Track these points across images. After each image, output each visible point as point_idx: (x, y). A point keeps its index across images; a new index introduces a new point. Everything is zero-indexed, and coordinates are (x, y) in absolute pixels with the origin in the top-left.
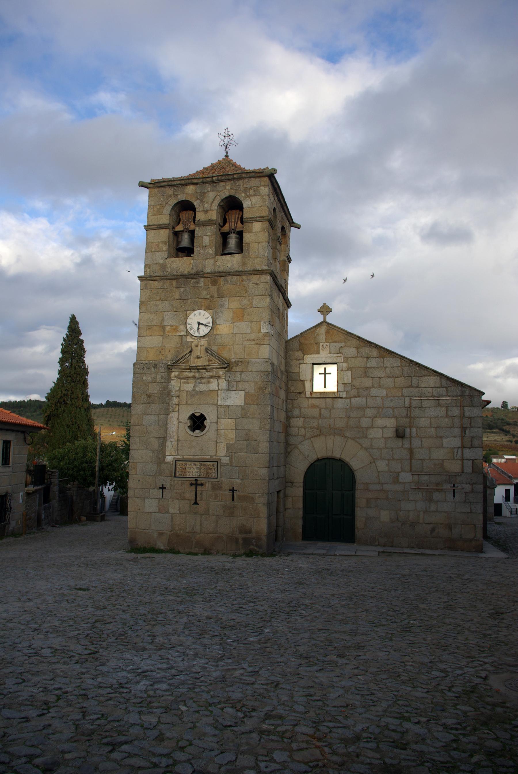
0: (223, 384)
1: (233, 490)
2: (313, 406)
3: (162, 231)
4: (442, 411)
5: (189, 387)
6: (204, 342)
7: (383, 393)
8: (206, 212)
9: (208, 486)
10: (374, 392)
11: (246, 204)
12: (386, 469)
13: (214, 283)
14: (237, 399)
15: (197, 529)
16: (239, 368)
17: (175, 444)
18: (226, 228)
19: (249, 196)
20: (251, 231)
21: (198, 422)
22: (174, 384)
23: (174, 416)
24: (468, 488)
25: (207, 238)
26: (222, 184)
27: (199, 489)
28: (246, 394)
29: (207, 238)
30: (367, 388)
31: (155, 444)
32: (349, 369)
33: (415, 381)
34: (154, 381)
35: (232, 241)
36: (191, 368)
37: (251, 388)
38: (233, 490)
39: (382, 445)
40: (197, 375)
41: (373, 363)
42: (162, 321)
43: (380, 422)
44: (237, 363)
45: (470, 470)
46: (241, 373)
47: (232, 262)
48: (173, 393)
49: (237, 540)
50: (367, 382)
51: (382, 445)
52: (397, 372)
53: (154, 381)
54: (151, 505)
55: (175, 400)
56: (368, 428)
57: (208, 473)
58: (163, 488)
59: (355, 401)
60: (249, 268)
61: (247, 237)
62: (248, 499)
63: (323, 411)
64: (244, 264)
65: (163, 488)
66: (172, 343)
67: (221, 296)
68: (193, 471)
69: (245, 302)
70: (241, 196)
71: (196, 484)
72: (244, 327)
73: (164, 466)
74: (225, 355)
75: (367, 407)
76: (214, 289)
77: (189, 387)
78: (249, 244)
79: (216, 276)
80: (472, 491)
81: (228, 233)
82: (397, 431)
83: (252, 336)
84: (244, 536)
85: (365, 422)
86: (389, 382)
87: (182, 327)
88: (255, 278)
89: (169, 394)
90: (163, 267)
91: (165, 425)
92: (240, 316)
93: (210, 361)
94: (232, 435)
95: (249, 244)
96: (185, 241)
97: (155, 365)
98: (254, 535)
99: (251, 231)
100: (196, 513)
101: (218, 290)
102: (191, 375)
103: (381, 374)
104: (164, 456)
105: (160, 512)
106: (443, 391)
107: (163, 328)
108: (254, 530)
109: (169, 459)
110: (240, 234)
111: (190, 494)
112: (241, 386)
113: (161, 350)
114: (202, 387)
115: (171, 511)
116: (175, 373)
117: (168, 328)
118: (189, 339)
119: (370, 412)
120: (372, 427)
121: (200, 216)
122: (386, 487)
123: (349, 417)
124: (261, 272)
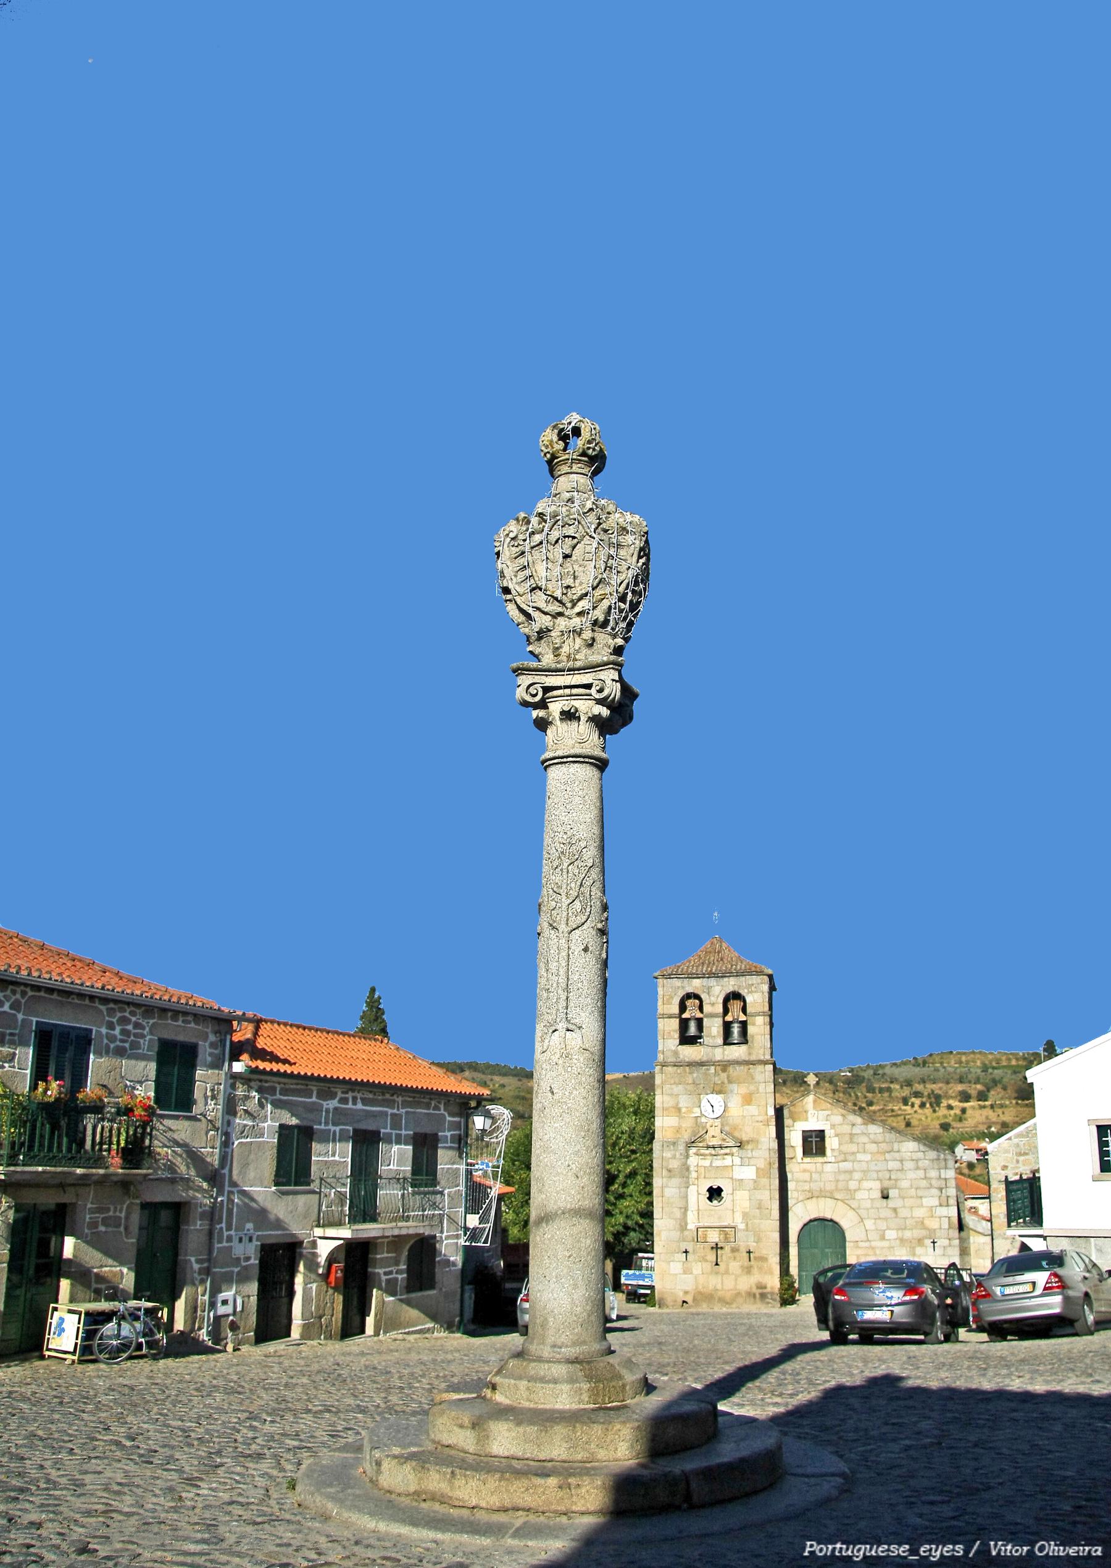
0: (737, 1160)
1: (749, 1252)
2: (805, 1171)
3: (673, 1020)
4: (921, 1173)
5: (707, 1163)
6: (718, 1122)
7: (868, 1157)
8: (713, 1004)
9: (727, 1249)
10: (860, 1157)
11: (749, 999)
12: (873, 1228)
13: (724, 1070)
14: (748, 1173)
15: (719, 1287)
16: (750, 1147)
17: (696, 1213)
18: (729, 1018)
19: (751, 992)
20: (754, 1024)
21: (715, 1193)
22: (693, 1161)
23: (692, 1189)
24: (946, 1242)
25: (713, 1028)
26: (726, 979)
27: (719, 1252)
28: (757, 1169)
29: (713, 1028)
30: (853, 1153)
31: (678, 1214)
32: (837, 1135)
33: (896, 1146)
34: (674, 1157)
35: (736, 1029)
36: (708, 1147)
37: (762, 1164)
38: (749, 1252)
39: (869, 1206)
40: (713, 1152)
41: (856, 1130)
42: (678, 1103)
43: (866, 1184)
44: (748, 1142)
45: (947, 1226)
46: (752, 1150)
47: (736, 1052)
48: (691, 1169)
49: (754, 1296)
50: (853, 1148)
51: (869, 1206)
52: (880, 1138)
53: (674, 1157)
54: (676, 1267)
55: (694, 1175)
56: (855, 1191)
57: (726, 1238)
58: (686, 1252)
59: (842, 1165)
60: (753, 1058)
61: (751, 1030)
62: (763, 1259)
63: (814, 1175)
64: (750, 1054)
65: (686, 1252)
66: (688, 1124)
67: (730, 1082)
68: (714, 1237)
69: (752, 1088)
70: (743, 992)
71: (716, 1247)
72: (752, 1110)
73: (686, 1233)
74: (737, 1134)
75: (854, 1171)
76: (724, 1075)
77: (707, 1163)
78: (753, 1036)
79: (725, 1065)
80: (950, 1245)
81: (731, 1022)
82: (882, 1192)
83: (760, 1118)
84: (760, 1291)
85: (853, 1185)
86: (873, 1147)
87: (697, 1110)
88: (760, 1068)
89: (688, 1169)
90: (676, 1053)
91: (686, 1197)
92: (748, 1100)
93: (724, 1140)
94: (747, 1204)
95: (753, 1036)
96: (692, 1030)
97: (674, 1143)
98: (769, 1290)
99: (754, 1024)
100: (717, 1273)
101: (728, 1077)
102: (707, 1152)
103: (864, 1139)
104: (686, 1224)
105: (685, 1272)
106: (921, 1155)
107: (679, 1110)
108: (769, 1286)
109: (691, 1226)
110: (744, 1025)
111: (711, 1257)
112: (752, 1162)
113: (678, 1130)
114: (718, 1163)
115: (695, 1272)
116: (693, 1151)
117: (684, 1110)
118: (703, 1120)
119: (857, 1176)
120: (859, 1189)
121: (707, 1008)
122: (873, 1244)
123: (838, 1181)
124: (765, 1063)
